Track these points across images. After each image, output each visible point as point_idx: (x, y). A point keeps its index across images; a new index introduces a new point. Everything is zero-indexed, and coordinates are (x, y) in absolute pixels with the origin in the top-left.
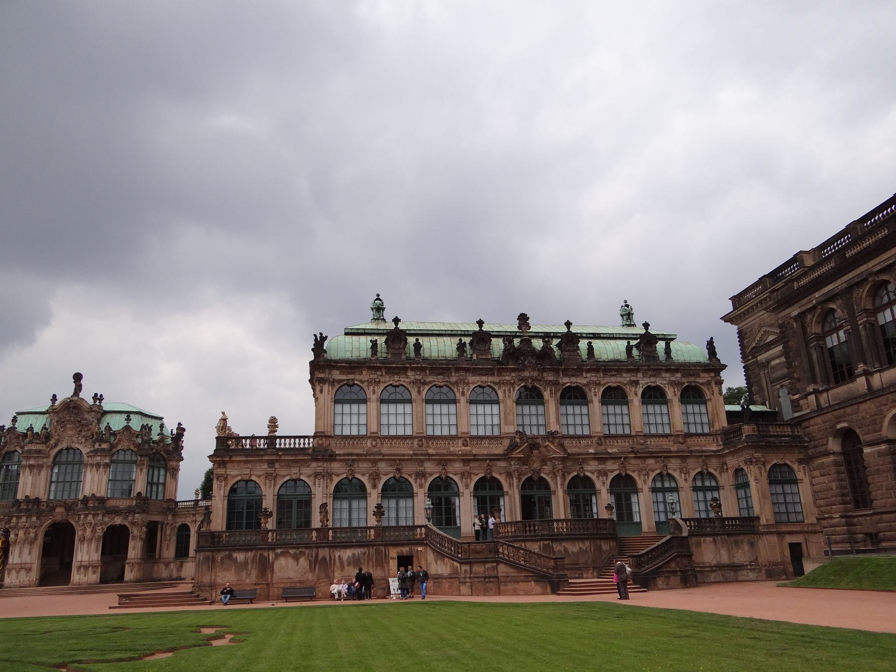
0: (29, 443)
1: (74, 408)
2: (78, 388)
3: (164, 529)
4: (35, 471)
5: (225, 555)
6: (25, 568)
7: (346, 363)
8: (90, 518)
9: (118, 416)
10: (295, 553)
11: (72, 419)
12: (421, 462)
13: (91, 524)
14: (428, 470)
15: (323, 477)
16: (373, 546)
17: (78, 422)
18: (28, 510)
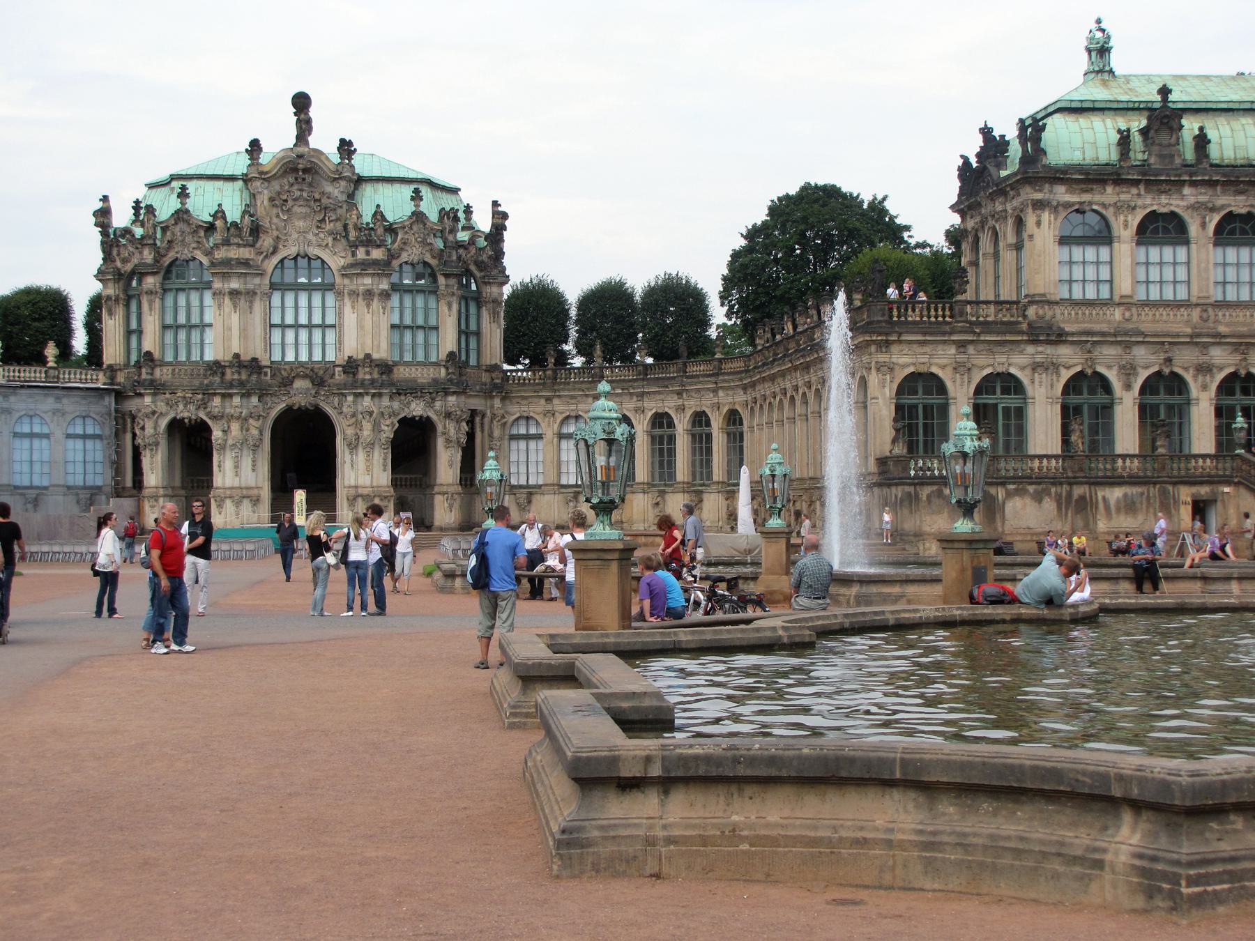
0: (223, 245)
1: (305, 171)
2: (304, 127)
3: (486, 427)
4: (243, 303)
5: (933, 492)
6: (244, 496)
7: (1080, 174)
8: (367, 401)
9: (386, 190)
10: (1035, 491)
11: (305, 194)
12: (1205, 346)
13: (371, 414)
14: (1217, 362)
15: (1047, 369)
16: (1155, 483)
17: (316, 200)
18: (242, 384)
